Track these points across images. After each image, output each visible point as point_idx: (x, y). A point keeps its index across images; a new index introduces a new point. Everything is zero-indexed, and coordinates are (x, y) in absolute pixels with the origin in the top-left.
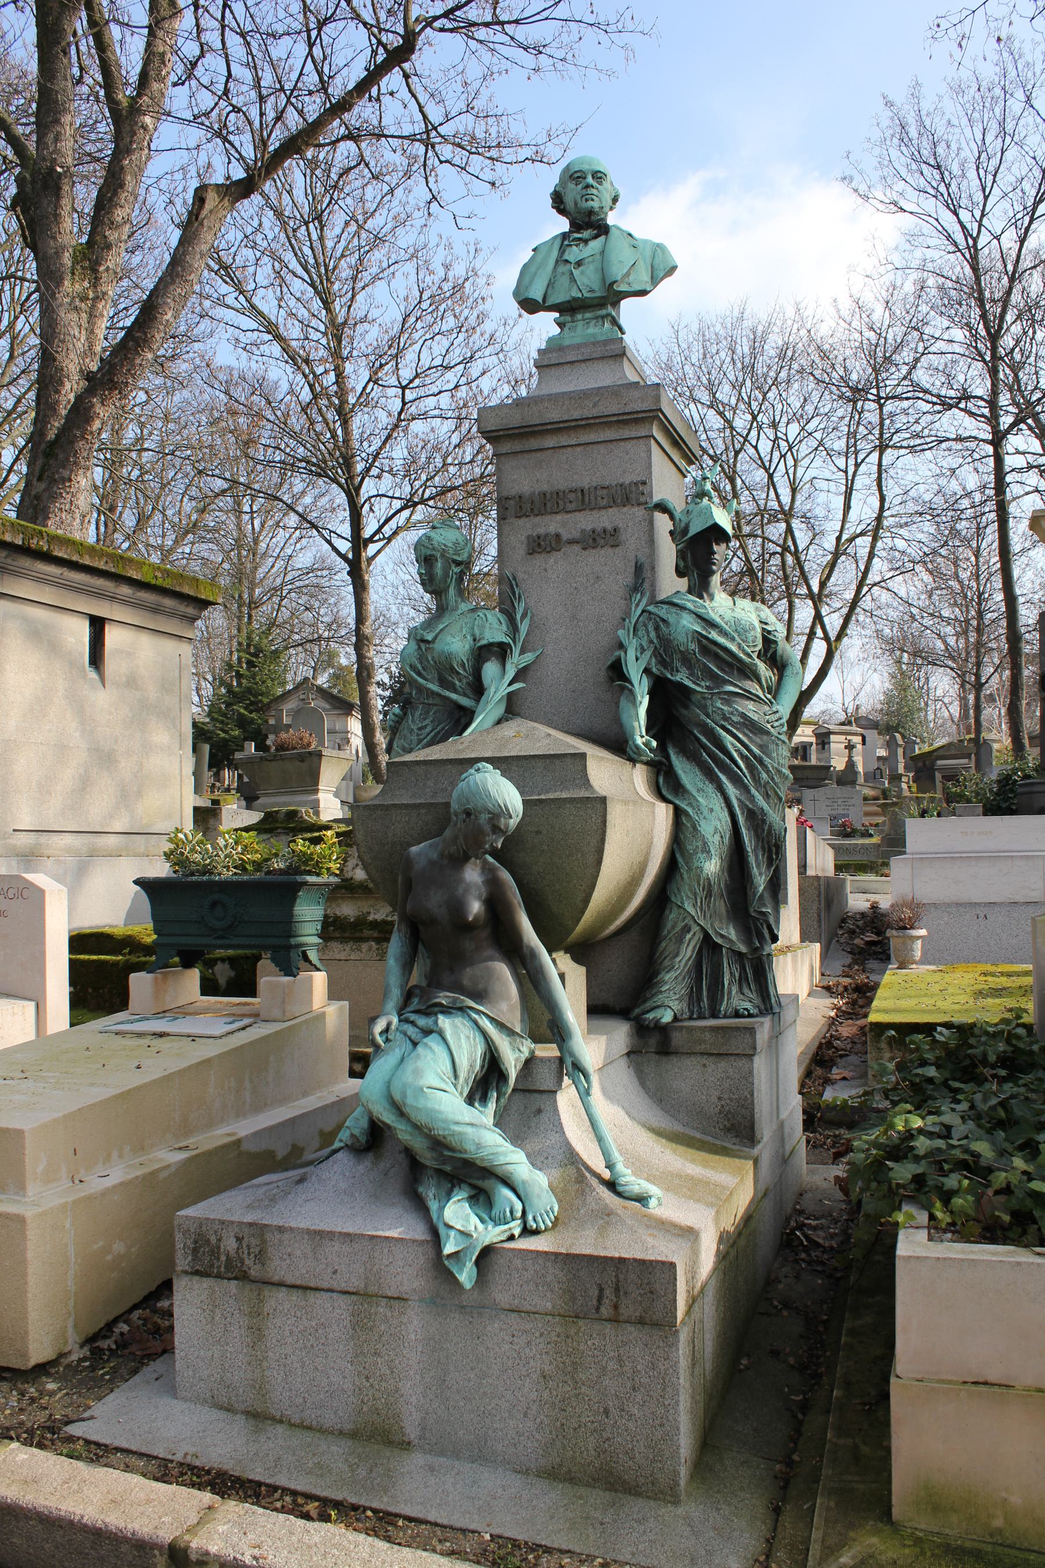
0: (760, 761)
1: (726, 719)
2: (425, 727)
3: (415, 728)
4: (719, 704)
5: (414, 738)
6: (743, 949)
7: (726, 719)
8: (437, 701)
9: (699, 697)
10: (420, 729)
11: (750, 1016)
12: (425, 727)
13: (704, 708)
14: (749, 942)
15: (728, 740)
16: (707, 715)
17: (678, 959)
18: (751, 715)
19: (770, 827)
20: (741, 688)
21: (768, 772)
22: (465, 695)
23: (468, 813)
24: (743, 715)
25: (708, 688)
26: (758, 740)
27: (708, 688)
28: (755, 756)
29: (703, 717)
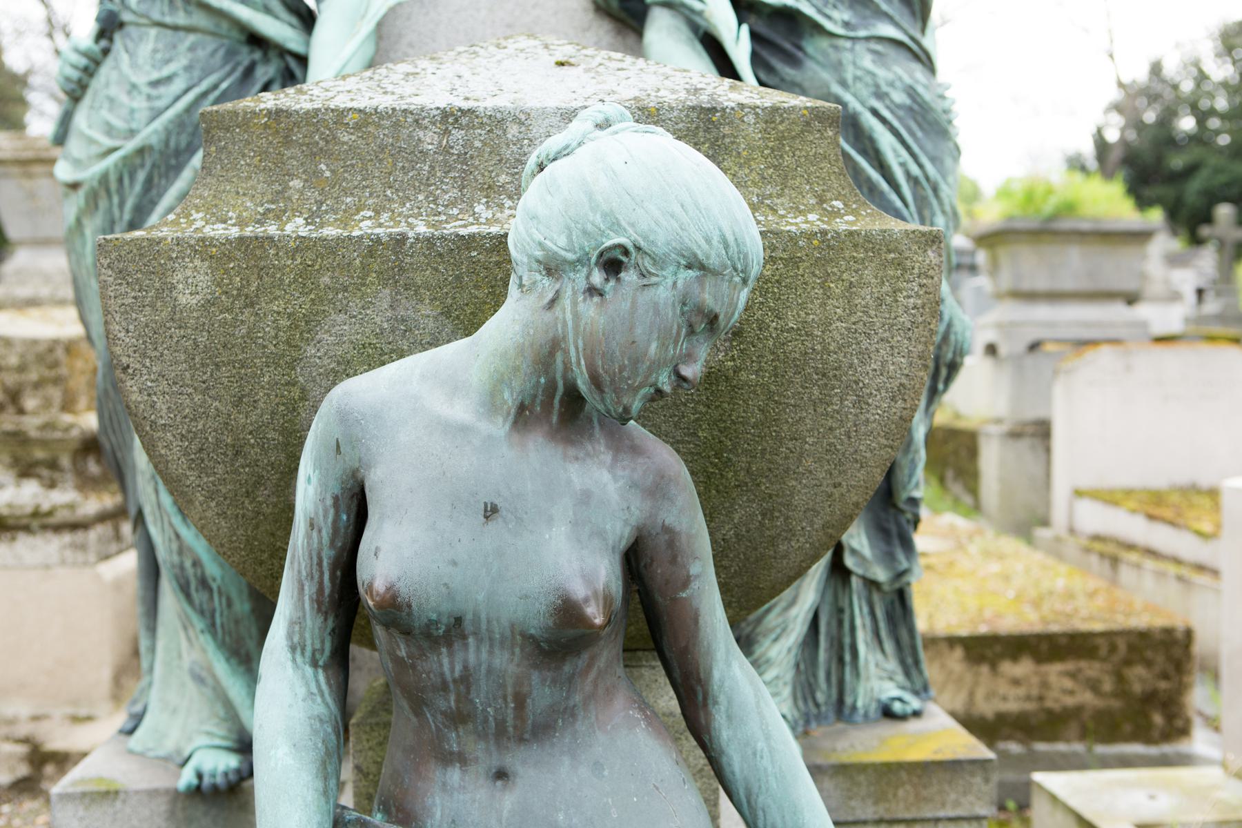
0: (935, 190)
1: (880, 95)
2: (169, 79)
3: (141, 80)
4: (867, 62)
5: (140, 103)
6: (881, 574)
7: (880, 95)
8: (199, 19)
9: (824, 43)
10: (155, 84)
11: (917, 714)
12: (169, 79)
13: (838, 67)
14: (889, 558)
15: (886, 141)
16: (843, 83)
17: (794, 611)
18: (920, 89)
19: (949, 326)
20: (906, 32)
21: (944, 212)
22: (267, 10)
23: (613, 264)
24: (911, 92)
25: (846, 25)
26: (929, 146)
27: (846, 25)
28: (927, 178)
29: (836, 89)
